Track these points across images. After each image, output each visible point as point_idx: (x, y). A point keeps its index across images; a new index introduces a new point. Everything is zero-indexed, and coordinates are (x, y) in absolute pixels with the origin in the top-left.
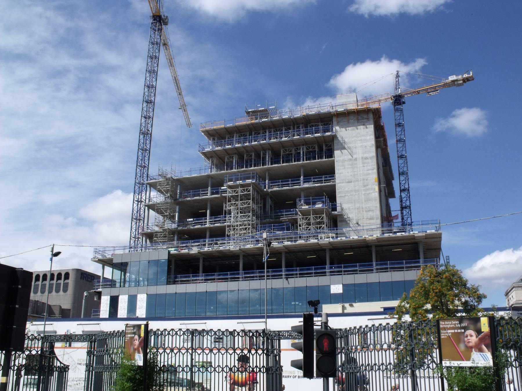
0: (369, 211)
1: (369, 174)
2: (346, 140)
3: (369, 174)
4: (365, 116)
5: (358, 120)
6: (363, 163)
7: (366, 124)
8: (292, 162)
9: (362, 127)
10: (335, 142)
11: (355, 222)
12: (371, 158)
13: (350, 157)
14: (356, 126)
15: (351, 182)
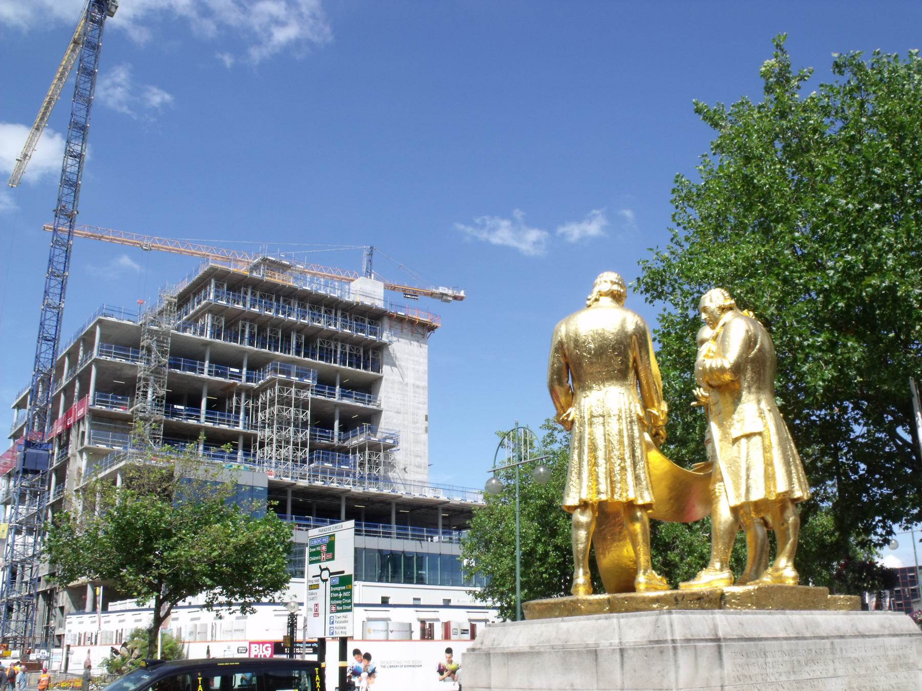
0: (417, 456)
1: (419, 408)
2: (398, 355)
3: (419, 408)
4: (420, 330)
5: (412, 332)
6: (414, 392)
7: (421, 341)
8: (331, 362)
9: (415, 343)
10: (385, 352)
11: (402, 467)
12: (423, 388)
13: (401, 380)
14: (410, 340)
15: (400, 413)
